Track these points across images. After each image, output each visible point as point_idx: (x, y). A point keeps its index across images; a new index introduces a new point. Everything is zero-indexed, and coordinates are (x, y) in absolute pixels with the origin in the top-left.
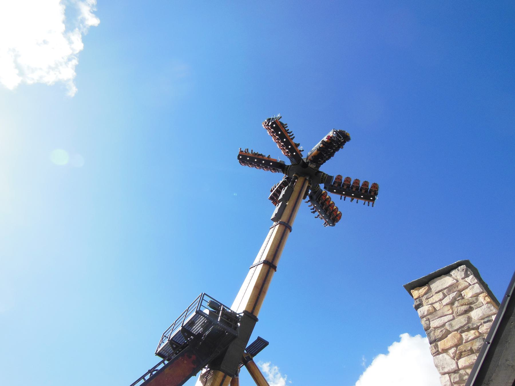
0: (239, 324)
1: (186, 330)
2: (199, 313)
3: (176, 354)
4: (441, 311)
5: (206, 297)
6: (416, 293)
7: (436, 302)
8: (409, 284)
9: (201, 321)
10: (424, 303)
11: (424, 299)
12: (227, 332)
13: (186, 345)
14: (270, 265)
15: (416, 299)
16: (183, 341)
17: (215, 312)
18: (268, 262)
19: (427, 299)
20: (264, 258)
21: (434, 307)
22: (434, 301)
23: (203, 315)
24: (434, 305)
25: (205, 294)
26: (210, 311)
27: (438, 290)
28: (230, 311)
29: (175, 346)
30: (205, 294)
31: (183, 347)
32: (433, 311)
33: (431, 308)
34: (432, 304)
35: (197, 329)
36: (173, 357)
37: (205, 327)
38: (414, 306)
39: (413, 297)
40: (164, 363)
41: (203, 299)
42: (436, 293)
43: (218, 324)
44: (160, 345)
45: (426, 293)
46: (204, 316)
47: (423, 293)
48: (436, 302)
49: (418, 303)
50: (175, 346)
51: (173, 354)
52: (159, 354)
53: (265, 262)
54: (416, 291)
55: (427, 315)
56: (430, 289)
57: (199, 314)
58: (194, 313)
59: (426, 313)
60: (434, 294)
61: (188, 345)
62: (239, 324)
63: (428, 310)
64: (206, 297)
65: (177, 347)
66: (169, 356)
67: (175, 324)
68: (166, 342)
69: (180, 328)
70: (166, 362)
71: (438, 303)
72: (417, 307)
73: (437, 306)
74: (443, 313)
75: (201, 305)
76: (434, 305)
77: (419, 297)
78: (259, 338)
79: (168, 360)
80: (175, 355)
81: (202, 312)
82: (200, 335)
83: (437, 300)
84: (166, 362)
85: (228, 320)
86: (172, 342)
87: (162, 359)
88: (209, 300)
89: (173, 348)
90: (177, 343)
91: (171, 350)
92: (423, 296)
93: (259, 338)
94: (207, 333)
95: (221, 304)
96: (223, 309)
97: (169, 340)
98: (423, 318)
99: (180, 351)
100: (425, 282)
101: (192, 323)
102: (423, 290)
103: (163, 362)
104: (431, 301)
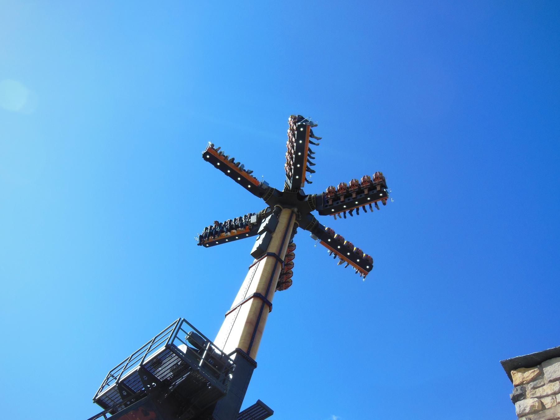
0: (231, 376)
1: (146, 371)
2: (171, 349)
3: (126, 405)
4: (552, 411)
5: (185, 326)
6: (518, 377)
7: (547, 396)
8: (511, 360)
9: (172, 361)
10: (528, 394)
11: (529, 387)
12: (210, 385)
13: (143, 394)
14: (263, 300)
15: (516, 386)
16: (139, 387)
17: (197, 351)
18: (260, 294)
19: (534, 388)
20: (253, 290)
21: (542, 403)
22: (545, 394)
23: (178, 352)
24: (543, 400)
25: (184, 320)
26: (189, 349)
27: (555, 376)
28: (219, 353)
29: (125, 394)
30: (184, 320)
31: (138, 397)
32: (540, 408)
33: (537, 404)
34: (540, 398)
35: (164, 372)
36: (120, 410)
37: (178, 371)
38: (511, 396)
39: (512, 381)
40: (105, 417)
41: (180, 328)
42: (551, 381)
43: (198, 370)
44: (103, 387)
45: (533, 380)
46: (177, 354)
47: (530, 378)
48: (547, 396)
49: (519, 392)
50: (125, 394)
51: (120, 404)
52: (99, 402)
53: (256, 296)
54: (520, 374)
55: (529, 413)
56: (541, 375)
57: (171, 350)
58: (163, 348)
59: (527, 410)
60: (546, 382)
61: (146, 395)
62: (231, 376)
63: (532, 406)
64: (185, 326)
65: (129, 394)
66: (114, 406)
67: (130, 359)
68: (113, 384)
69: (137, 367)
70: (109, 415)
71: (550, 398)
72: (516, 399)
73: (547, 402)
74: (554, 414)
75: (175, 336)
76: (543, 400)
77: (522, 384)
78: (259, 403)
79: (111, 413)
80: (123, 406)
81: (176, 347)
82: (167, 383)
83: (550, 393)
84: (109, 415)
85: (215, 367)
86: (122, 386)
87: (102, 410)
88: (189, 330)
89: (122, 394)
90: (130, 389)
91: (118, 398)
92: (528, 383)
93: (259, 403)
94: (179, 381)
95: (208, 341)
96: (210, 348)
97: (117, 383)
98: (522, 416)
99: (132, 403)
100: (537, 361)
101: (157, 361)
102: (530, 374)
103: (103, 414)
104: (539, 392)
